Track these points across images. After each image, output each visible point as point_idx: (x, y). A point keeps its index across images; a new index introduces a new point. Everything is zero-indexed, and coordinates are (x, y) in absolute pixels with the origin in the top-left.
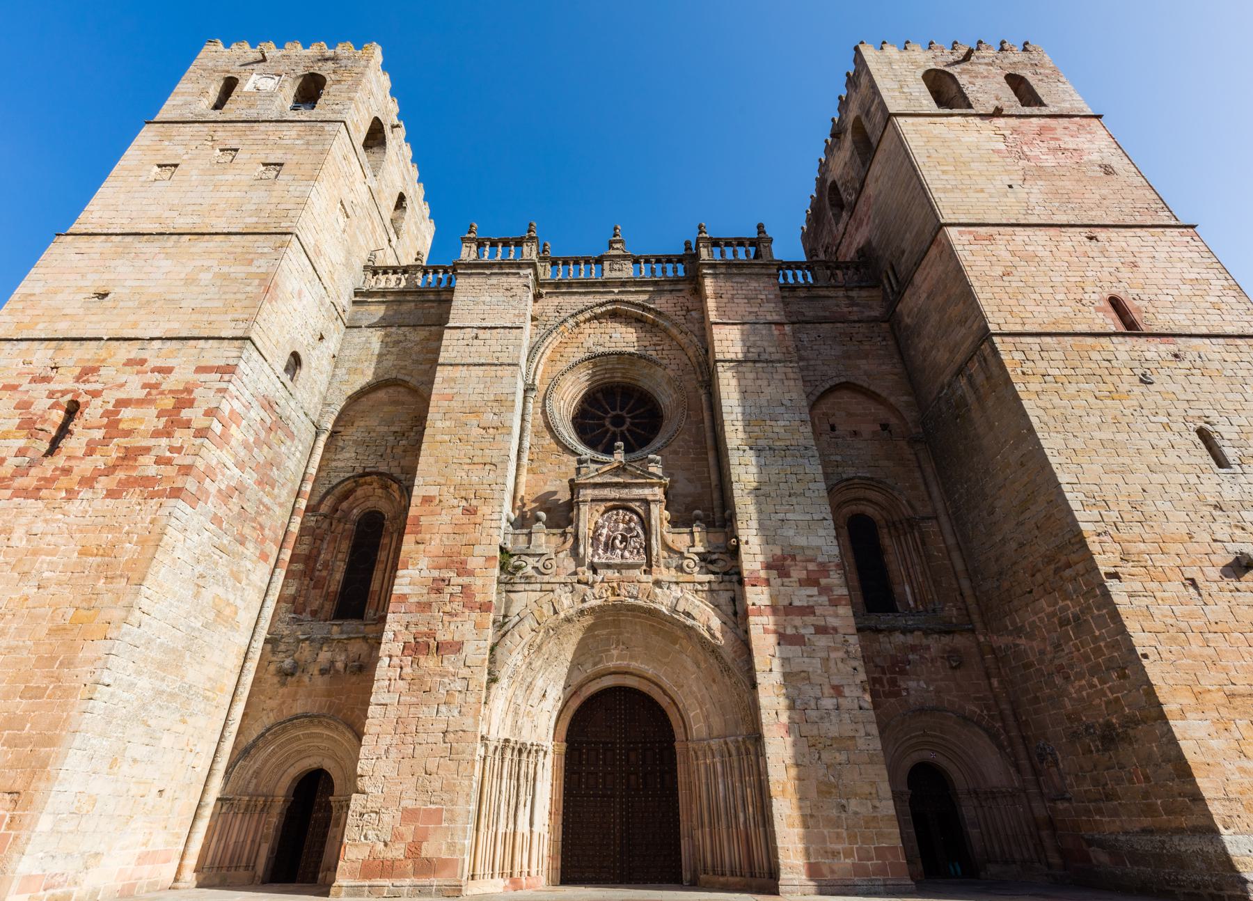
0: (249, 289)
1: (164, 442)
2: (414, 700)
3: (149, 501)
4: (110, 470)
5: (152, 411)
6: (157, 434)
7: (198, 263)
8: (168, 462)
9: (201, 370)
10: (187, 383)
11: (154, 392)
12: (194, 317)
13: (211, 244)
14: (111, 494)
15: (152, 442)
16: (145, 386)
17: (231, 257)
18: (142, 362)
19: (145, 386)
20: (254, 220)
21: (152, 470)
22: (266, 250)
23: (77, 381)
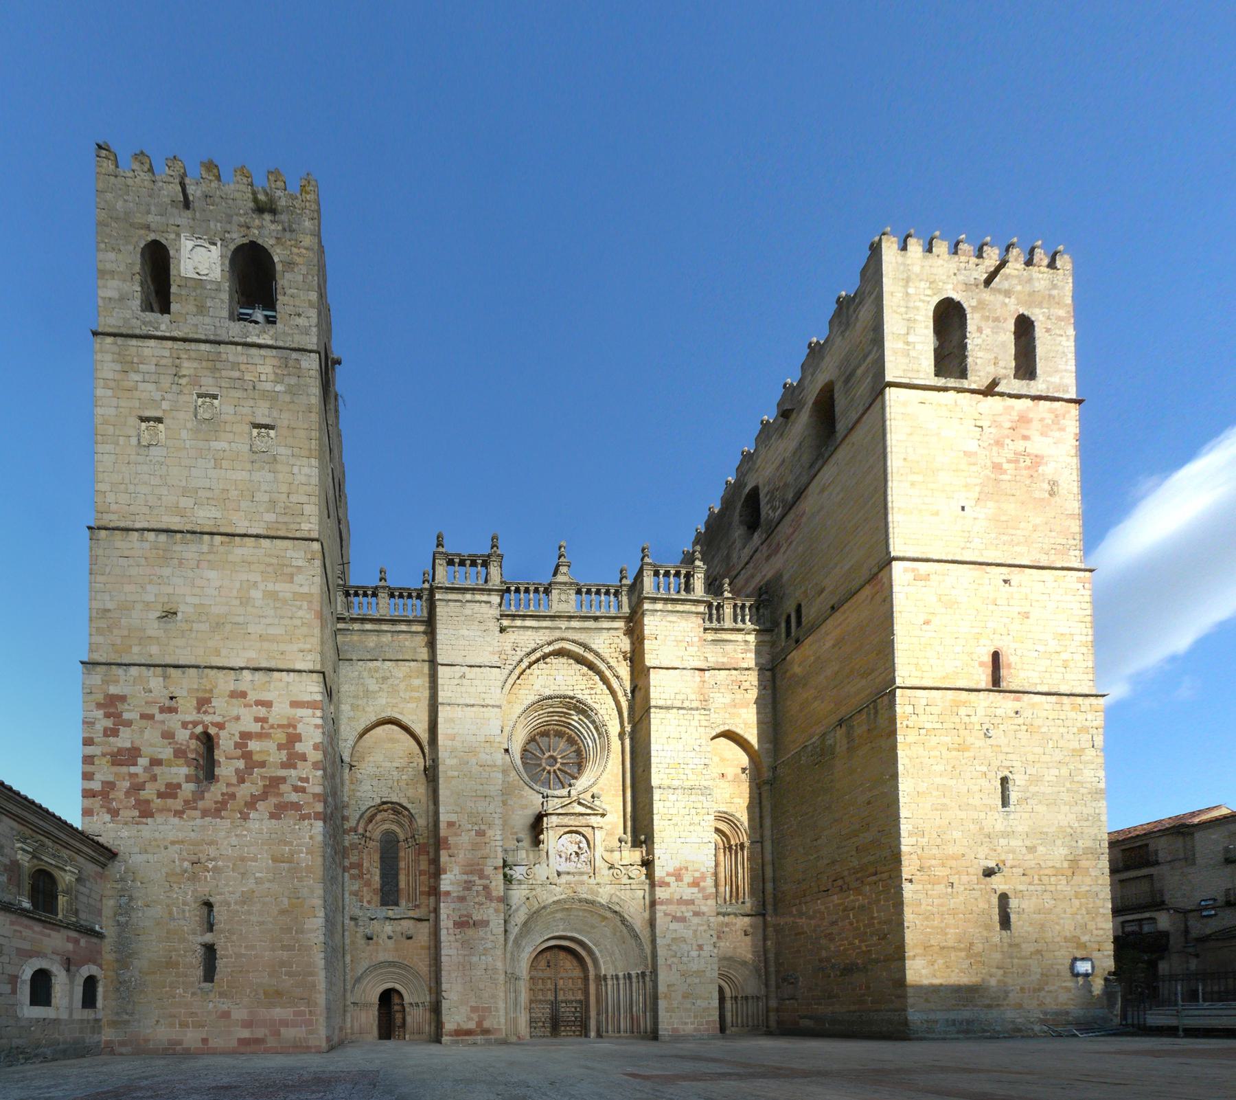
0: (300, 613)
1: (293, 772)
2: (466, 953)
3: (302, 821)
4: (264, 796)
5: (271, 746)
6: (284, 766)
7: (244, 577)
8: (303, 790)
9: (295, 704)
10: (288, 718)
11: (266, 725)
12: (266, 645)
13: (245, 551)
14: (273, 816)
15: (282, 773)
16: (257, 720)
17: (270, 569)
18: (243, 695)
19: (257, 720)
20: (270, 517)
21: (294, 797)
22: (300, 563)
23: (199, 712)
